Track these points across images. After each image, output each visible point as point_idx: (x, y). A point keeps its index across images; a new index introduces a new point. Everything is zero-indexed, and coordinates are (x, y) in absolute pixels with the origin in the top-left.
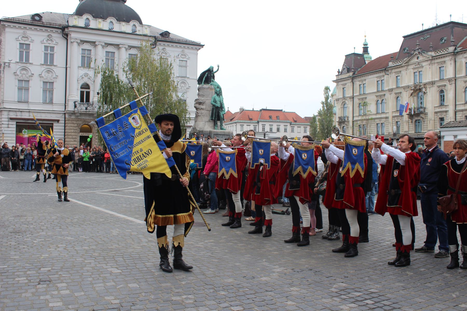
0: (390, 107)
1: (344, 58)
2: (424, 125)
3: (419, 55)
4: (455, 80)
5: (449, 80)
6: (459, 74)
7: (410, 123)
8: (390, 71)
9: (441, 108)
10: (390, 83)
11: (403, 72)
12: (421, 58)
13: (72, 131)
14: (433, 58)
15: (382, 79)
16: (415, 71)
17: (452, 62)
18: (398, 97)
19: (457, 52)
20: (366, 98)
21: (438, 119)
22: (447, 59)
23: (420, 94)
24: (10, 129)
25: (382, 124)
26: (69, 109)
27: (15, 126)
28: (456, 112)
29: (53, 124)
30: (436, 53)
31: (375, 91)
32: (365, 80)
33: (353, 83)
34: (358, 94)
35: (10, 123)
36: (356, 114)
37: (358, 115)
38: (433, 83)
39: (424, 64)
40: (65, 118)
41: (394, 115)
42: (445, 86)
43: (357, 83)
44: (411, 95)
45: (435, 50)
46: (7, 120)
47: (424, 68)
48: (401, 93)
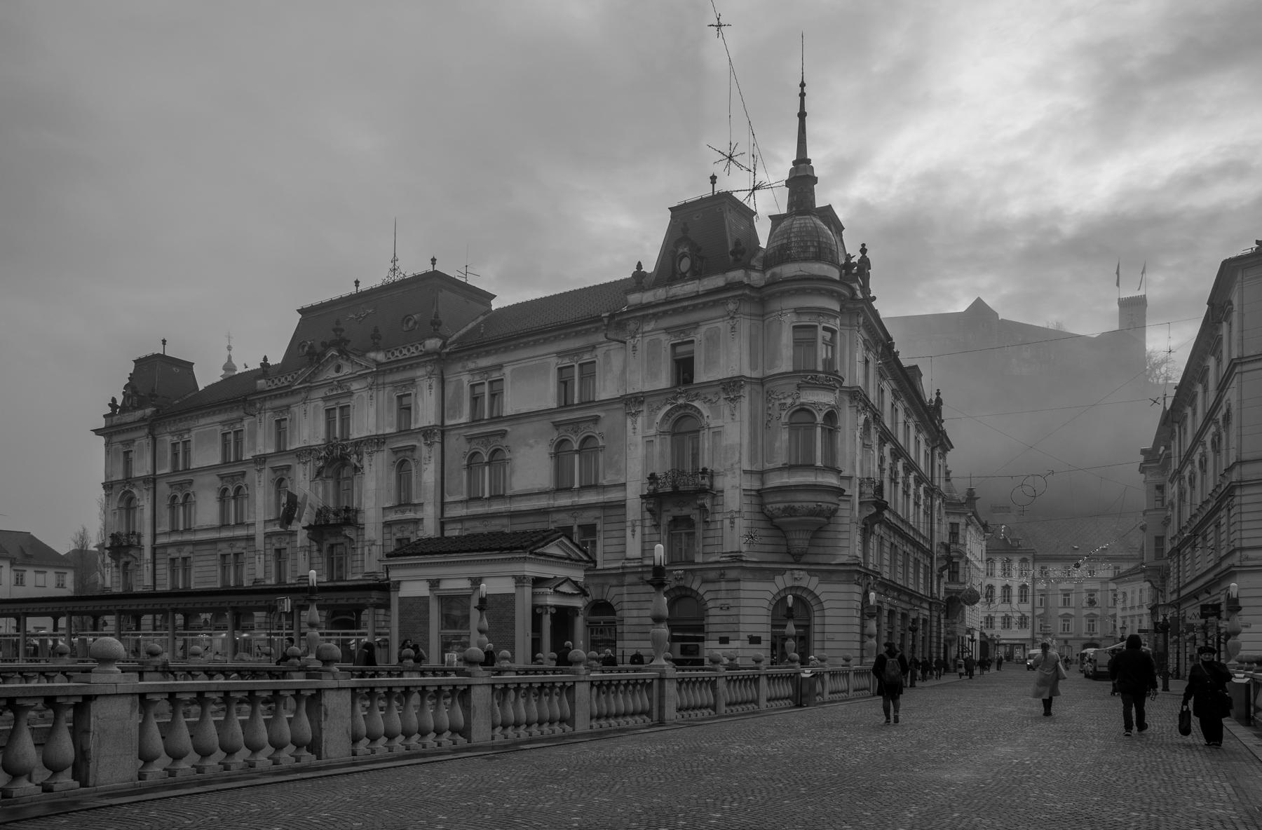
0: (261, 505)
1: (131, 368)
3: (341, 361)
4: (443, 433)
5: (426, 432)
6: (453, 417)
7: (315, 554)
8: (258, 405)
9: (403, 512)
10: (260, 440)
11: (294, 409)
12: (347, 370)
14: (382, 369)
15: (238, 427)
16: (331, 404)
17: (435, 382)
18: (281, 480)
19: (448, 354)
20: (191, 482)
22: (420, 372)
23: (346, 472)
25: (236, 555)
30: (390, 355)
31: (217, 460)
32: (189, 430)
33: (154, 439)
34: (167, 470)
36: (164, 526)
37: (167, 529)
38: (378, 441)
39: (355, 386)
41: (269, 530)
42: (413, 448)
43: (167, 440)
44: (319, 473)
47: (355, 397)
48: (289, 467)
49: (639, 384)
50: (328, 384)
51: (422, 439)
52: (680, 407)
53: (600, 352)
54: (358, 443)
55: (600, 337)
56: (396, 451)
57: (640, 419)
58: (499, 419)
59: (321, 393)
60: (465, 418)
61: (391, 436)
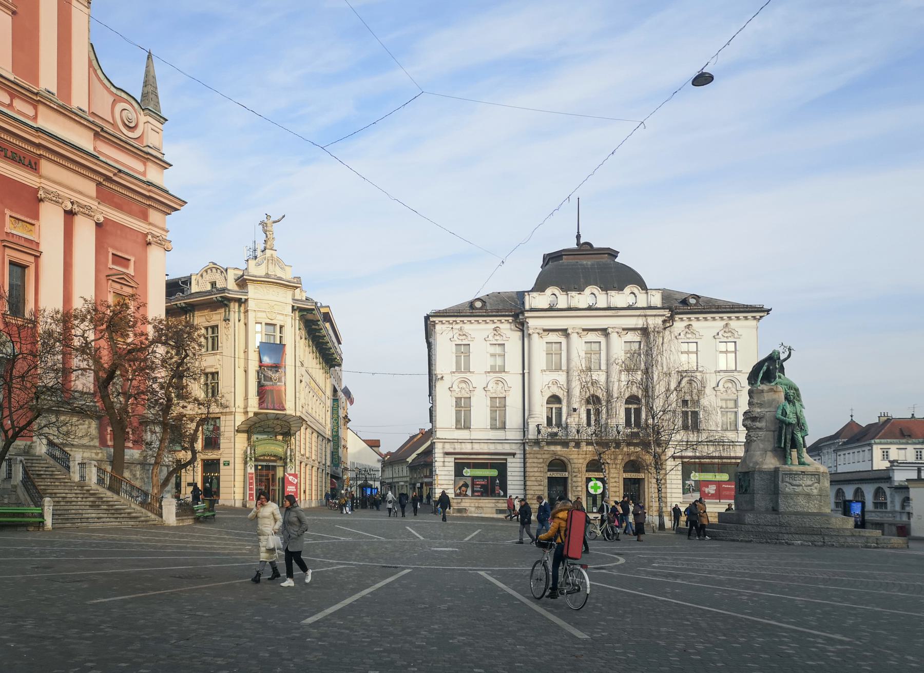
13: (536, 469)
24: (446, 468)
26: (530, 437)
27: (453, 464)
29: (506, 459)
35: (446, 460)
40: (524, 450)
46: (442, 455)
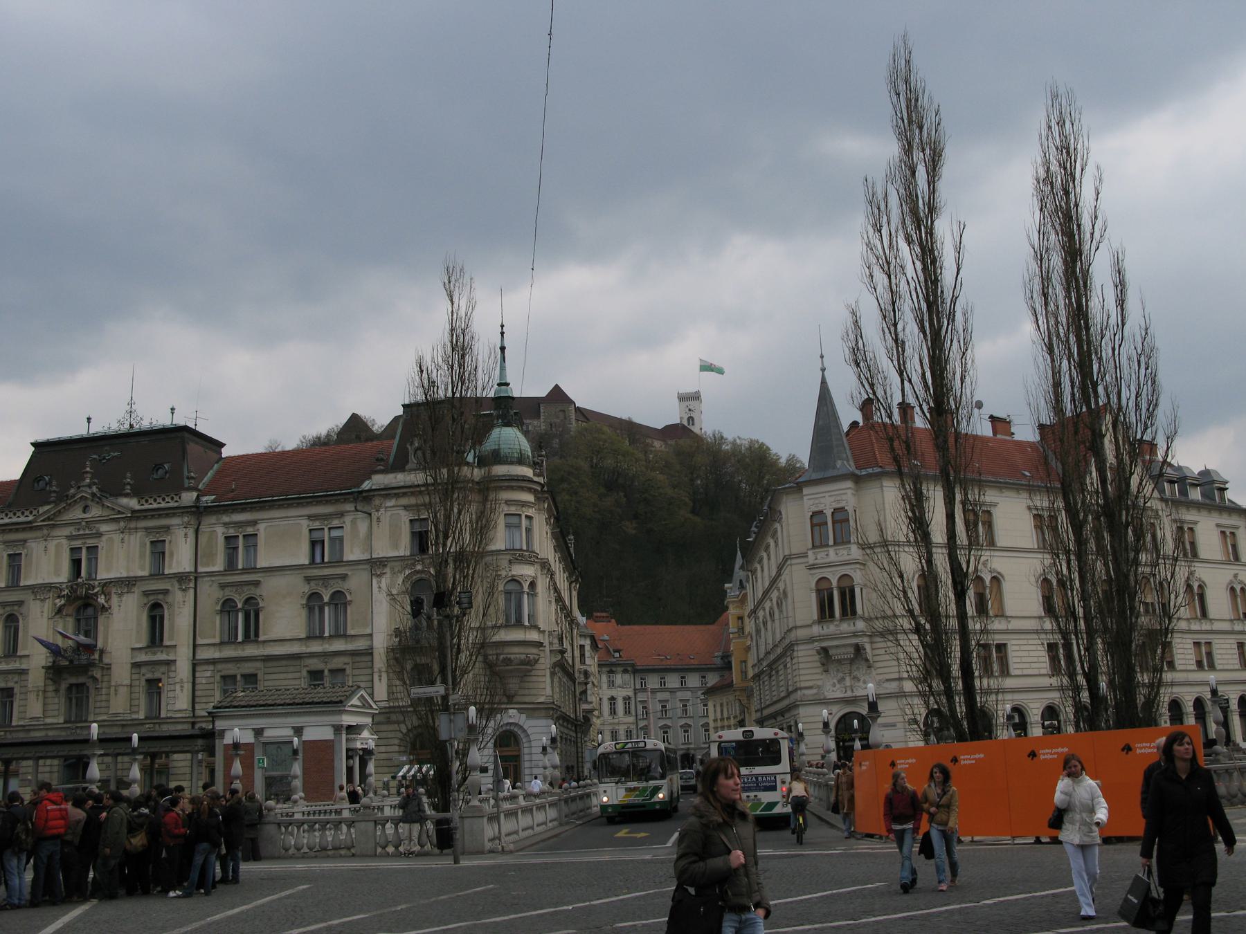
2: (99, 698)
5: (181, 578)
6: (207, 565)
9: (155, 653)
11: (32, 545)
14: (136, 515)
17: (191, 532)
21: (143, 683)
22: (175, 521)
28: (194, 666)
38: (128, 583)
39: (104, 528)
42: (166, 592)
45: (137, 493)
47: (104, 538)
49: (382, 550)
50: (76, 524)
51: (177, 585)
52: (418, 572)
53: (348, 519)
54: (106, 584)
55: (349, 507)
56: (146, 594)
57: (383, 580)
58: (254, 570)
59: (67, 531)
60: (219, 566)
61: (142, 578)
